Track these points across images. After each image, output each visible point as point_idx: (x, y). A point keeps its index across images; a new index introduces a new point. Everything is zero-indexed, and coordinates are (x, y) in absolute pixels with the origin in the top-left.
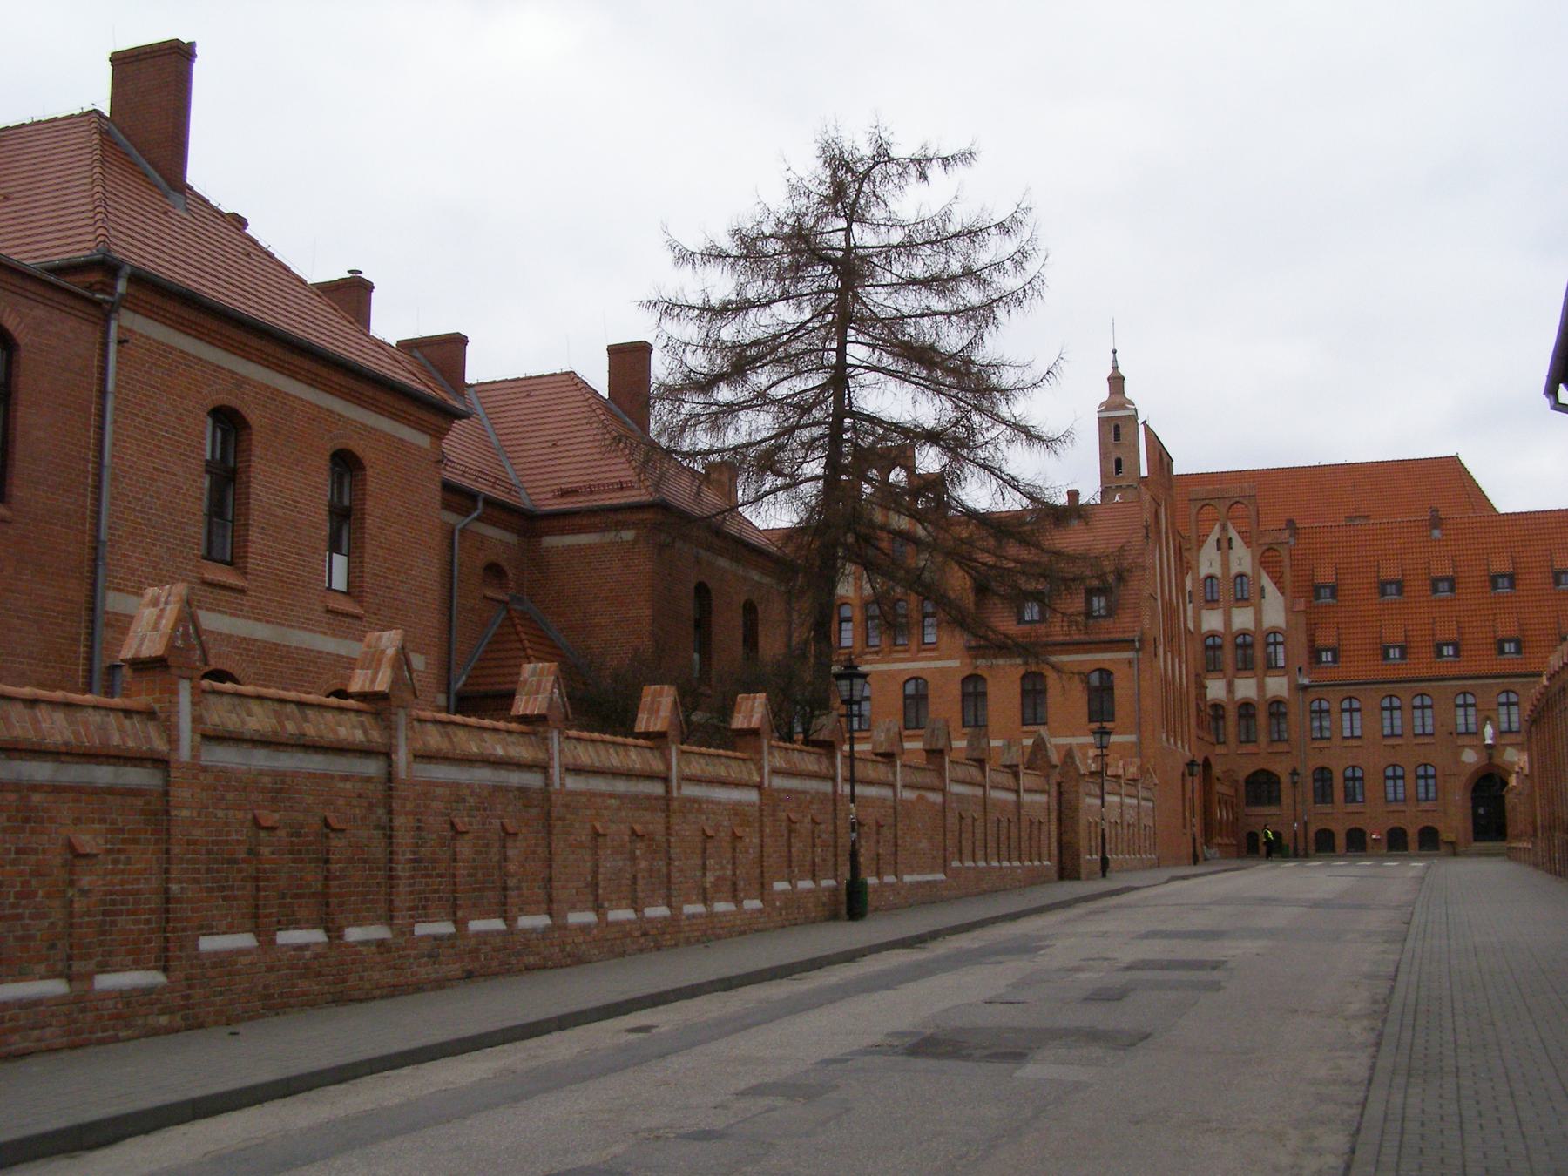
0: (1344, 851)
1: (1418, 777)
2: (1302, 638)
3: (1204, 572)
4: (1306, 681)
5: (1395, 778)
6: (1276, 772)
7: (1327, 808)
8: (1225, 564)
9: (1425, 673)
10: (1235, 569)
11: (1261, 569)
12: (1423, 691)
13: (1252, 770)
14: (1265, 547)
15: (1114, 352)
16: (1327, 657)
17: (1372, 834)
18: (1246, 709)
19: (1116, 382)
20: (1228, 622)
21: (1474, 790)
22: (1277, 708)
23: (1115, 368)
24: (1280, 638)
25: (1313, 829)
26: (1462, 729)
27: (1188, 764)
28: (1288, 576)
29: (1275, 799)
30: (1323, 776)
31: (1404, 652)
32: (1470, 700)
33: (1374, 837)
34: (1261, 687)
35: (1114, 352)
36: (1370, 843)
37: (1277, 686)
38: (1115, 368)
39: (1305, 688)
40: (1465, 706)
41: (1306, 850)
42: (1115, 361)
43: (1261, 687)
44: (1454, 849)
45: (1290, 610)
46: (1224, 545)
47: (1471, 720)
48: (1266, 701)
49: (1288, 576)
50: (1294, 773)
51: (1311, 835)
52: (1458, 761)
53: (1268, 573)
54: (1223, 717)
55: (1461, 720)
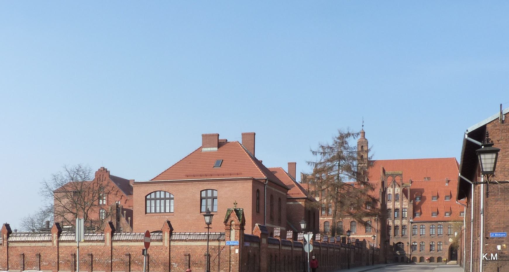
10: (396, 192)
23: (363, 129)
24: (406, 210)
28: (409, 195)
33: (426, 259)
39: (412, 223)
49: (409, 195)
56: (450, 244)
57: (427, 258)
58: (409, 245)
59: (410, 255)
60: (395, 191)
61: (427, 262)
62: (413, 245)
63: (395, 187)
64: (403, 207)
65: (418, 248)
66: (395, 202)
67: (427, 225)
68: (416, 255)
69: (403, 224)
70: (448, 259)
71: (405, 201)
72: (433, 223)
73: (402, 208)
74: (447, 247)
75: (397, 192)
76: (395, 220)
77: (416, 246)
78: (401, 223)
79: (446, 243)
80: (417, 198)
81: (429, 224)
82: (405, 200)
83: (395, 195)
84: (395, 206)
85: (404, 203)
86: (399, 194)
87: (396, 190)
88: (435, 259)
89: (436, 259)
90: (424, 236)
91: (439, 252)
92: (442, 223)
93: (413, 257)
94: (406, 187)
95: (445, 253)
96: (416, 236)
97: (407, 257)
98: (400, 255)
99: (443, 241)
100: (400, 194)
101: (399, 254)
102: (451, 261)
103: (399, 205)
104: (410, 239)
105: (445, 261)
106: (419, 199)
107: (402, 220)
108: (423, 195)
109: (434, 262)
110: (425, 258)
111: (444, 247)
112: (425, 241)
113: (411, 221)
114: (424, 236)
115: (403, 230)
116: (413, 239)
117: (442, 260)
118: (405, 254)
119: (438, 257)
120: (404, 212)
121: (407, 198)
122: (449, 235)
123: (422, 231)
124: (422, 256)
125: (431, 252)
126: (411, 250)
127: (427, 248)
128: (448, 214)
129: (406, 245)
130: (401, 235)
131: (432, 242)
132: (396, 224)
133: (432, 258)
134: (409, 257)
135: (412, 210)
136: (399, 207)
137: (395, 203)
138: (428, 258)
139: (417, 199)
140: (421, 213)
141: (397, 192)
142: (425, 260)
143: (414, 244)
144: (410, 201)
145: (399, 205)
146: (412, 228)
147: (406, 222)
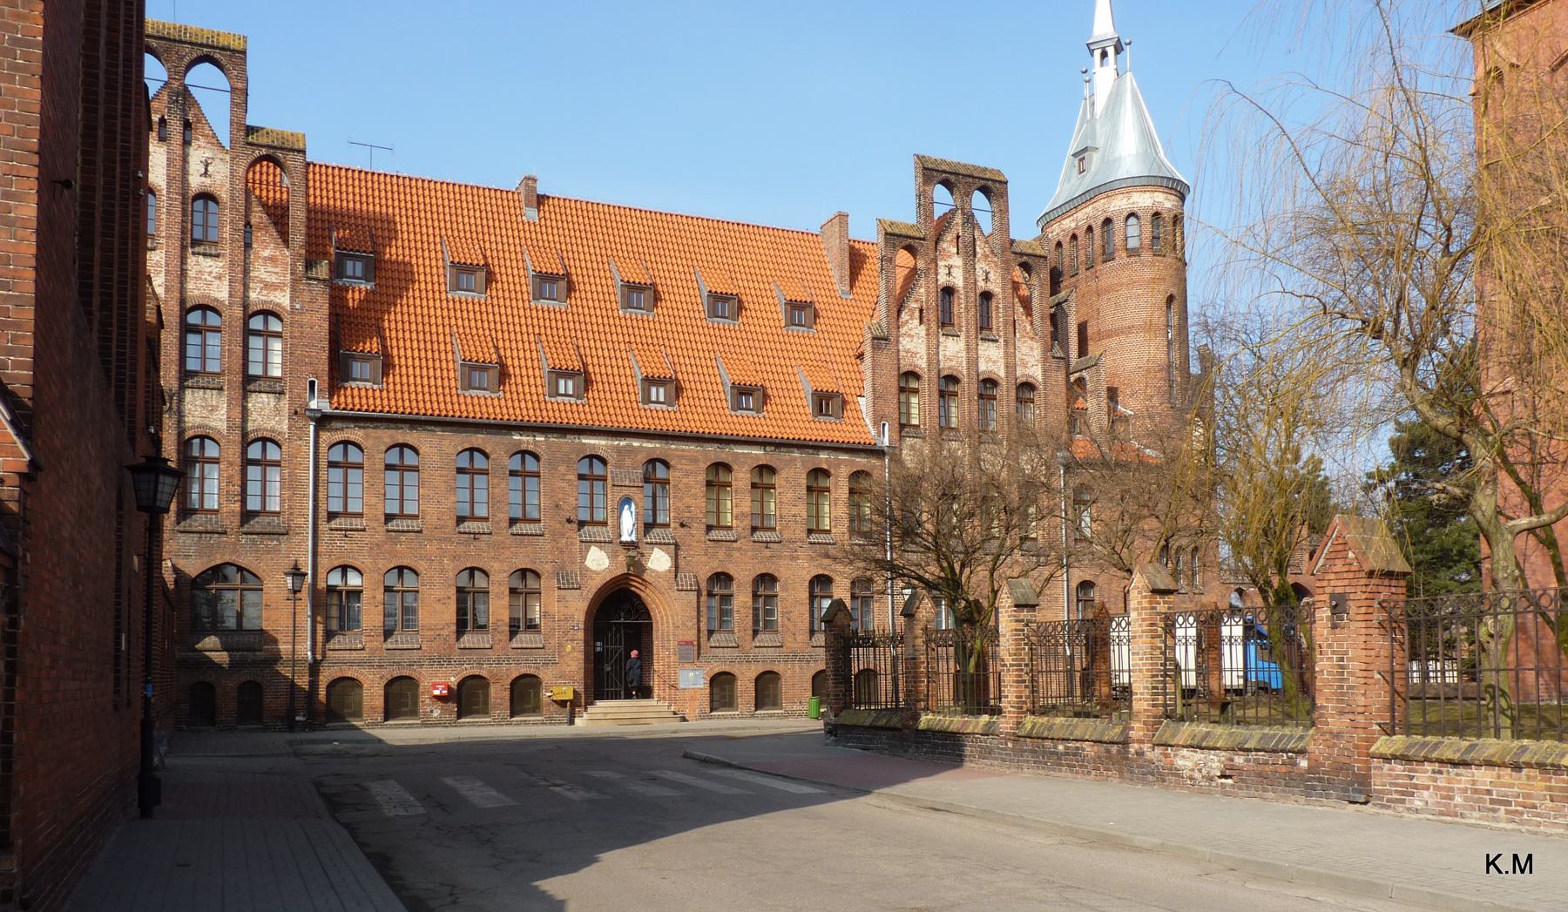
4: (326, 407)
9: (531, 415)
10: (196, 182)
21: (595, 619)
24: (275, 326)
39: (323, 421)
56: (595, 585)
57: (436, 680)
58: (305, 595)
59: (314, 668)
60: (185, 172)
61: (436, 714)
62: (331, 589)
63: (186, 143)
64: (253, 295)
65: (370, 614)
66: (183, 248)
67: (436, 448)
68: (360, 664)
69: (250, 426)
70: (581, 689)
71: (272, 259)
72: (479, 440)
73: (245, 307)
74: (577, 607)
75: (207, 181)
76: (188, 393)
77: (355, 594)
78: (238, 421)
79: (567, 583)
80: (349, 264)
81: (452, 443)
82: (266, 247)
83: (184, 195)
84: (190, 285)
85: (260, 272)
86: (224, 195)
87: (195, 167)
88: (493, 690)
89: (499, 694)
90: (414, 525)
91: (524, 639)
92: (536, 442)
93: (332, 685)
94: (280, 154)
95: (561, 646)
96: (357, 523)
97: (293, 685)
98: (232, 663)
99: (548, 567)
100: (233, 199)
101: (221, 657)
102: (599, 703)
103: (219, 278)
104: (310, 543)
105: (562, 703)
106: (359, 274)
107: (245, 397)
108: (392, 252)
109: (484, 711)
110: (425, 683)
111: (555, 608)
112: (421, 566)
113: (314, 405)
114: (414, 525)
115: (254, 472)
116: (335, 547)
117: (537, 694)
118: (276, 658)
119: (515, 675)
121: (286, 242)
122: (582, 524)
123: (397, 489)
124: (406, 672)
125: (469, 640)
126: (320, 628)
127: (437, 610)
128: (570, 383)
129: (277, 584)
130: (237, 507)
132: (198, 421)
133: (528, 680)
134: (303, 681)
135: (326, 325)
136: (220, 292)
137: (191, 260)
138: (449, 688)
139: (349, 272)
140: (387, 366)
141: (207, 181)
142: (425, 699)
143: (335, 579)
144: (309, 265)
145: (219, 278)
147: (278, 411)
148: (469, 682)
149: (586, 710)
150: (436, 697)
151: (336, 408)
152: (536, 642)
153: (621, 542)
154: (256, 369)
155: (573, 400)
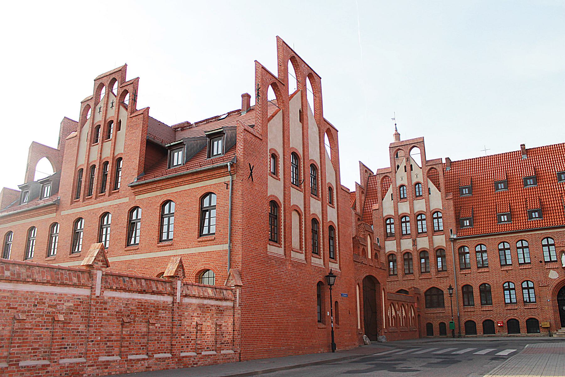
0: (482, 333)
1: (523, 289)
2: (451, 213)
3: (399, 183)
4: (455, 237)
5: (509, 289)
6: (441, 288)
7: (470, 309)
8: (410, 179)
9: (522, 228)
10: (414, 181)
11: (428, 179)
12: (523, 238)
13: (428, 288)
14: (429, 167)
15: (396, 125)
16: (467, 223)
17: (498, 323)
18: (423, 253)
19: (397, 135)
20: (412, 208)
21: (558, 296)
22: (440, 252)
23: (396, 130)
25: (463, 320)
26: (547, 259)
27: (327, 276)
28: (442, 181)
29: (441, 304)
30: (467, 290)
31: (511, 216)
32: (551, 241)
33: (499, 325)
34: (431, 242)
35: (396, 125)
36: (497, 329)
37: (440, 241)
38: (396, 130)
40: (548, 245)
41: (460, 333)
42: (396, 128)
43: (431, 242)
44: (550, 332)
45: (445, 198)
46: (408, 168)
47: (553, 253)
48: (434, 249)
49: (442, 181)
50: (450, 288)
51: (463, 325)
52: (546, 277)
53: (431, 180)
54: (412, 259)
55: (546, 254)
70: (553, 321)
102: (562, 329)
113: (452, 237)
120: (435, 221)
131: (509, 282)
146: (457, 255)
148: (530, 320)
149: (557, 331)
150: (499, 326)
151: (458, 237)
152: (530, 306)
153: (562, 268)
154: (436, 229)
155: (538, 219)
